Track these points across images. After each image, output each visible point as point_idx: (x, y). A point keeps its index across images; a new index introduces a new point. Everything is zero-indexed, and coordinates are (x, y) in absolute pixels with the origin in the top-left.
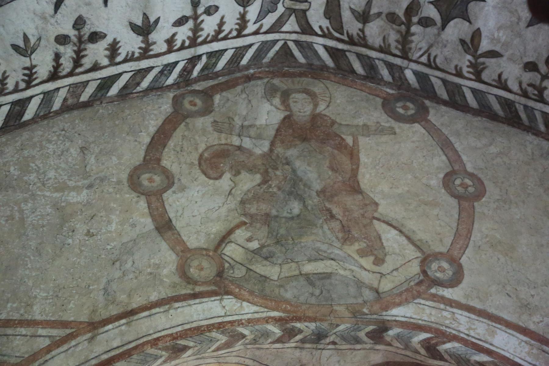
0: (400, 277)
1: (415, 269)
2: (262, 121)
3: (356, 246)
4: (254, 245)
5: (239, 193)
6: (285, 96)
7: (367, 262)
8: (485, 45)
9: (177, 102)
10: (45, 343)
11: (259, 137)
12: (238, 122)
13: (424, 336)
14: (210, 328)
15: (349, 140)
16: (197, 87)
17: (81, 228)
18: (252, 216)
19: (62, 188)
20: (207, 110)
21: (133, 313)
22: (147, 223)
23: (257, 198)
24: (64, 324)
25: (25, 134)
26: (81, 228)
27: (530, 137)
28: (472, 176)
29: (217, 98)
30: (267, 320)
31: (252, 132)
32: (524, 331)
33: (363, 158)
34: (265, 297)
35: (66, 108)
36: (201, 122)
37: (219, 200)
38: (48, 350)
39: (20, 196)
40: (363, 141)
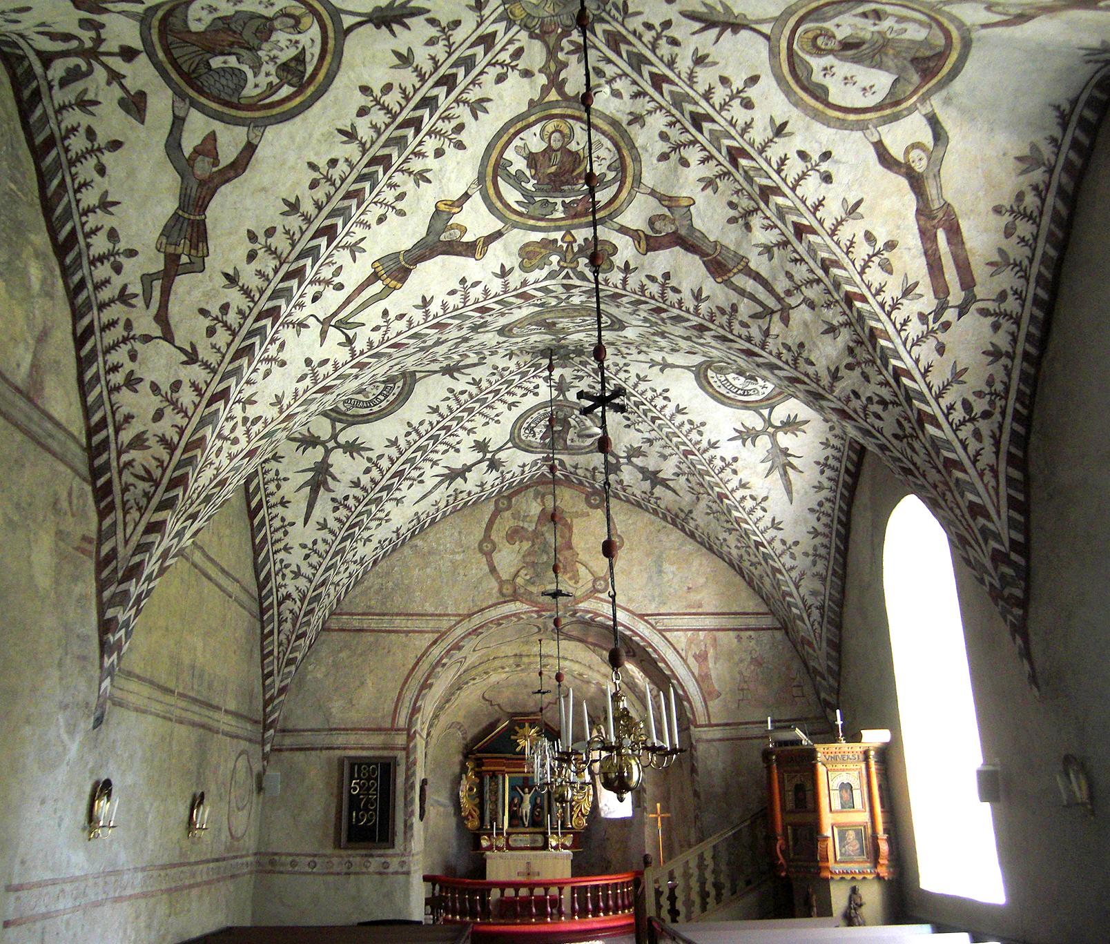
0: (584, 589)
1: (590, 585)
2: (532, 513)
3: (568, 575)
4: (528, 577)
5: (522, 551)
6: (543, 497)
7: (572, 583)
8: (625, 484)
9: (496, 502)
10: (453, 623)
11: (531, 522)
12: (522, 513)
13: (590, 615)
14: (511, 616)
15: (569, 521)
16: (505, 494)
17: (462, 572)
18: (527, 563)
19: (453, 553)
20: (509, 507)
21: (483, 610)
22: (486, 568)
23: (529, 554)
24: (460, 615)
25: (437, 526)
26: (462, 572)
27: (647, 514)
28: (619, 536)
29: (514, 499)
30: (532, 612)
31: (528, 519)
32: (628, 610)
33: (575, 530)
34: (532, 602)
35: (451, 513)
36: (507, 514)
37: (514, 555)
38: (455, 625)
39: (438, 558)
40: (575, 521)
